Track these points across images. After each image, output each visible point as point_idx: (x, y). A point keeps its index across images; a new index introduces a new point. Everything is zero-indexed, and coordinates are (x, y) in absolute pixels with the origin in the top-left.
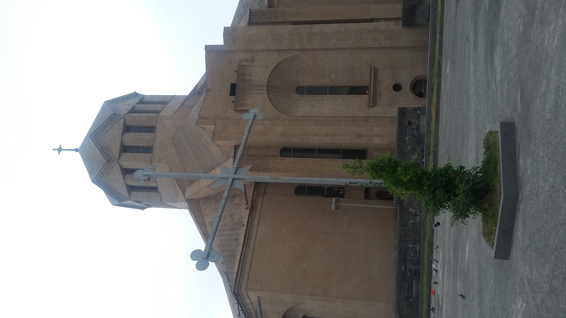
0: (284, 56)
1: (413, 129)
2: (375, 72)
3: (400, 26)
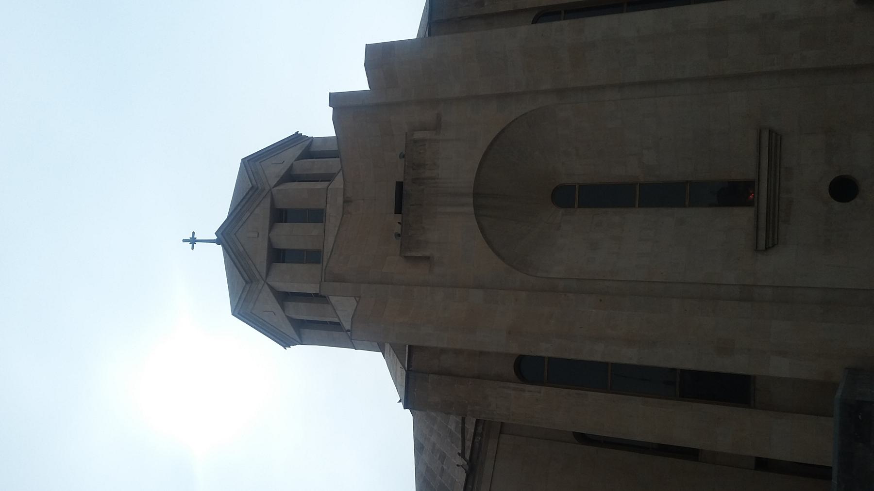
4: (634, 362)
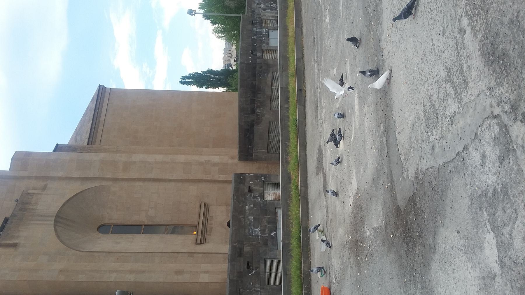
0: (89, 185)
1: (255, 197)
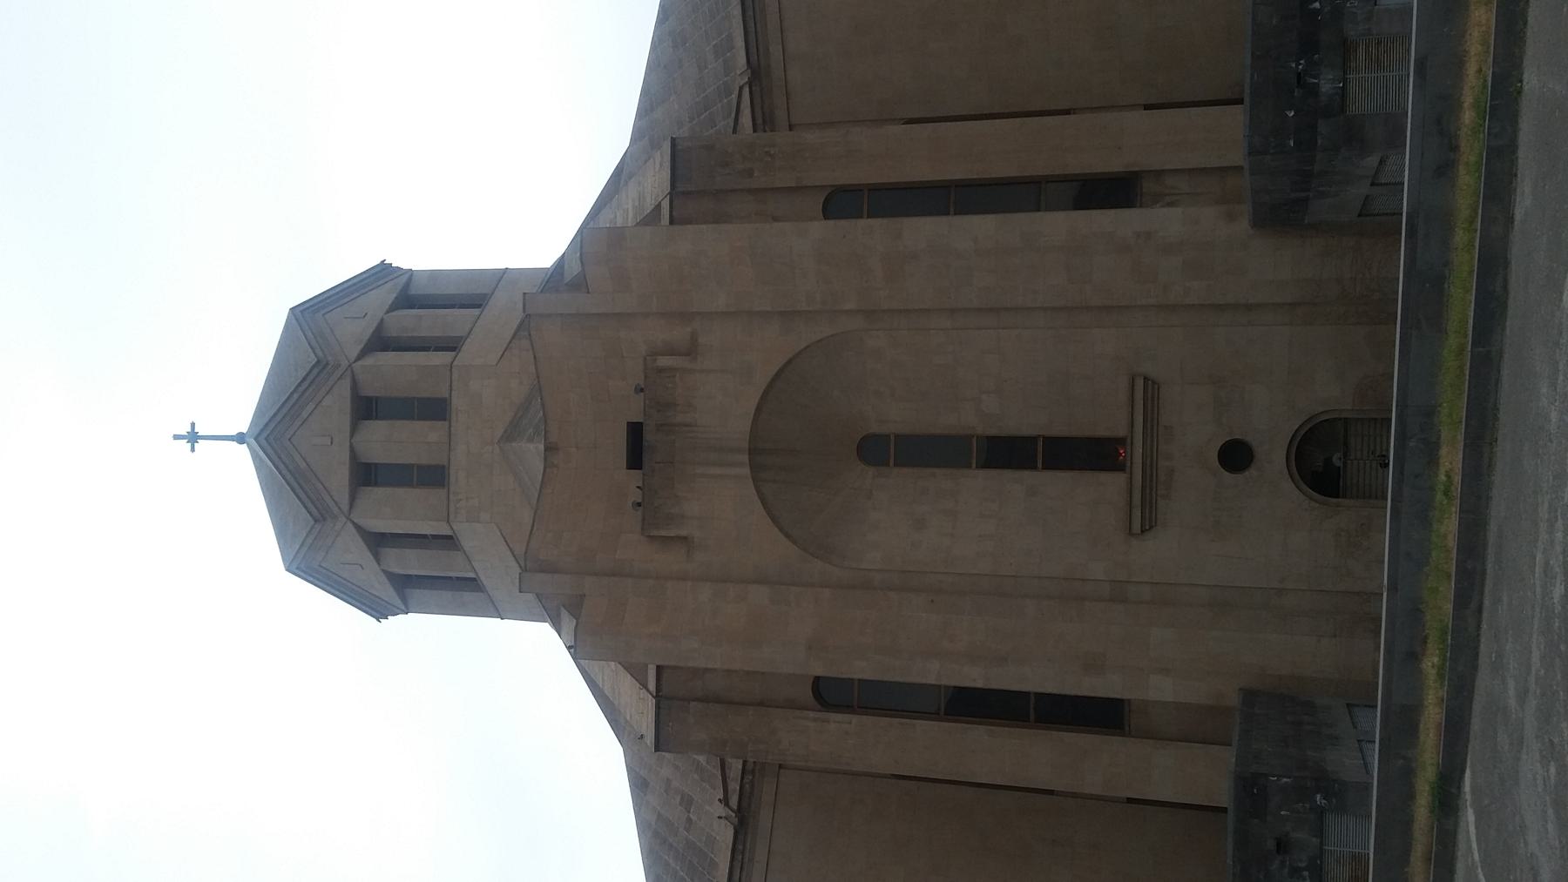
1: (1295, 871)
2: (1149, 392)
3: (1243, 225)
4: (980, 684)
